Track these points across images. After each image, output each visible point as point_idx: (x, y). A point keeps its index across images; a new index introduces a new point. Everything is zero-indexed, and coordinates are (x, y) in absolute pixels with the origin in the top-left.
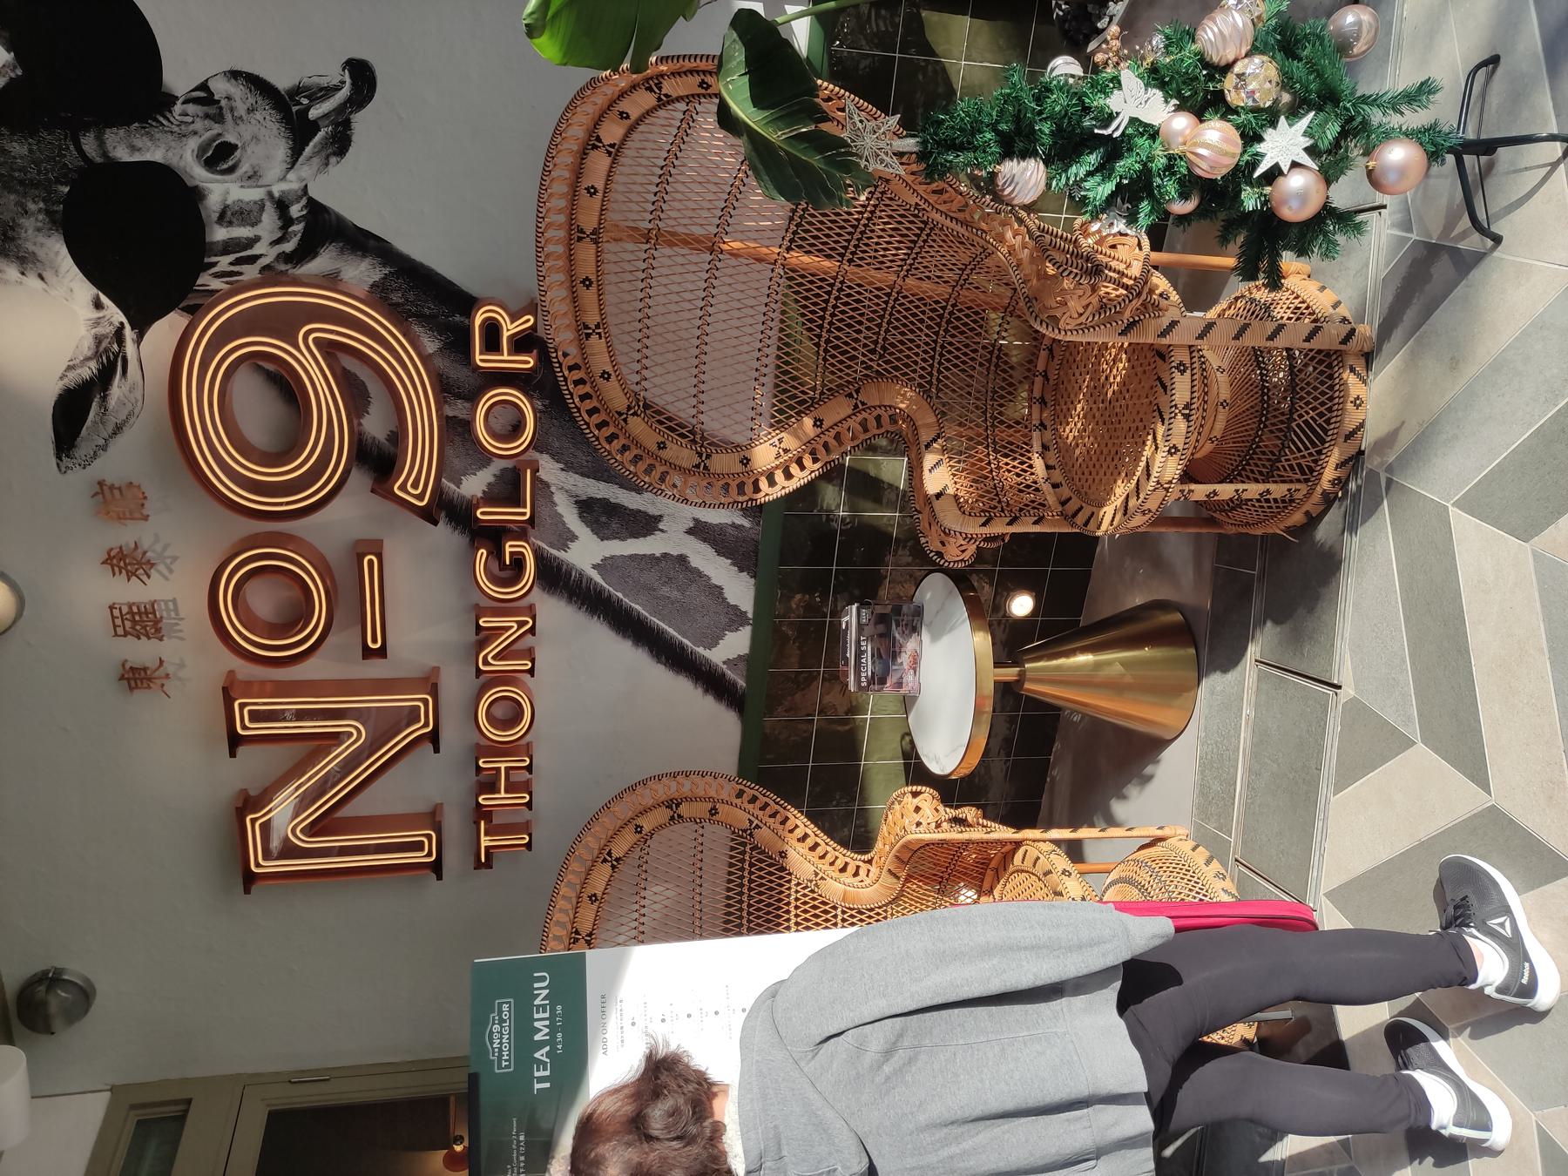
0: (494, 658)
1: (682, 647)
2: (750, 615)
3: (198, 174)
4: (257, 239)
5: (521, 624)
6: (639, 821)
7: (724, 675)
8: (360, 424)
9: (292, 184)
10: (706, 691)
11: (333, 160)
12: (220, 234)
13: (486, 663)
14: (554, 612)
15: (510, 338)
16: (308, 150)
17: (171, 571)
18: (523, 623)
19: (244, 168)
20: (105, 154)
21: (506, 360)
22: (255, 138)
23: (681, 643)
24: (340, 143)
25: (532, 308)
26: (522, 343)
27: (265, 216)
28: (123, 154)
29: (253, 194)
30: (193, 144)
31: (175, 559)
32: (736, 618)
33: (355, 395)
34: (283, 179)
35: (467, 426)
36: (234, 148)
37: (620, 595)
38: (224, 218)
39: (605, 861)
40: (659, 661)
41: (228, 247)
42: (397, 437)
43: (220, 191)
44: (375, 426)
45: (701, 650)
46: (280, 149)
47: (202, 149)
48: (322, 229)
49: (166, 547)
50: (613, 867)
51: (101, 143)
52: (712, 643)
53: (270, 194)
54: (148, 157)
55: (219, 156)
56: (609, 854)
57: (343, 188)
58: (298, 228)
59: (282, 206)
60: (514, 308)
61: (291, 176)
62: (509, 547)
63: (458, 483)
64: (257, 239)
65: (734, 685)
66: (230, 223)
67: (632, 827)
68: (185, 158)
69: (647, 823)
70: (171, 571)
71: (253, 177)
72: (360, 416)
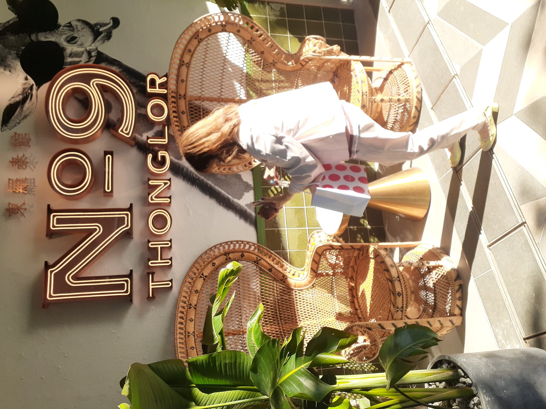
0: (155, 197)
1: (229, 199)
2: (252, 186)
3: (65, 44)
4: (81, 61)
5: (165, 184)
6: (214, 261)
7: (246, 211)
8: (108, 116)
9: (93, 47)
10: (240, 218)
11: (106, 41)
12: (69, 60)
13: (152, 199)
14: (178, 185)
15: (159, 84)
16: (99, 39)
17: (35, 168)
18: (165, 184)
19: (79, 43)
20: (37, 39)
21: (157, 90)
22: (83, 36)
23: (228, 197)
24: (109, 36)
25: (166, 76)
26: (162, 86)
27: (84, 55)
28: (43, 39)
29: (81, 49)
30: (64, 36)
31: (37, 163)
32: (247, 187)
33: (108, 107)
34: (90, 46)
35: (146, 116)
36: (76, 38)
37: (203, 178)
38: (71, 55)
39: (201, 277)
40: (220, 205)
41: (71, 63)
42: (120, 121)
43: (70, 48)
44: (113, 116)
45: (236, 200)
46: (91, 38)
47: (67, 38)
48: (101, 59)
49: (34, 158)
50: (204, 279)
51: (37, 36)
52: (240, 198)
53: (86, 50)
54: (50, 40)
55: (72, 40)
56: (202, 274)
57: (108, 49)
58: (94, 59)
59: (89, 53)
60: (160, 76)
61: (93, 45)
62: (160, 154)
63: (141, 136)
64: (81, 61)
65: (251, 215)
66: (73, 57)
67: (211, 264)
68: (62, 40)
69: (217, 262)
70: (35, 168)
71: (81, 45)
72: (109, 113)
